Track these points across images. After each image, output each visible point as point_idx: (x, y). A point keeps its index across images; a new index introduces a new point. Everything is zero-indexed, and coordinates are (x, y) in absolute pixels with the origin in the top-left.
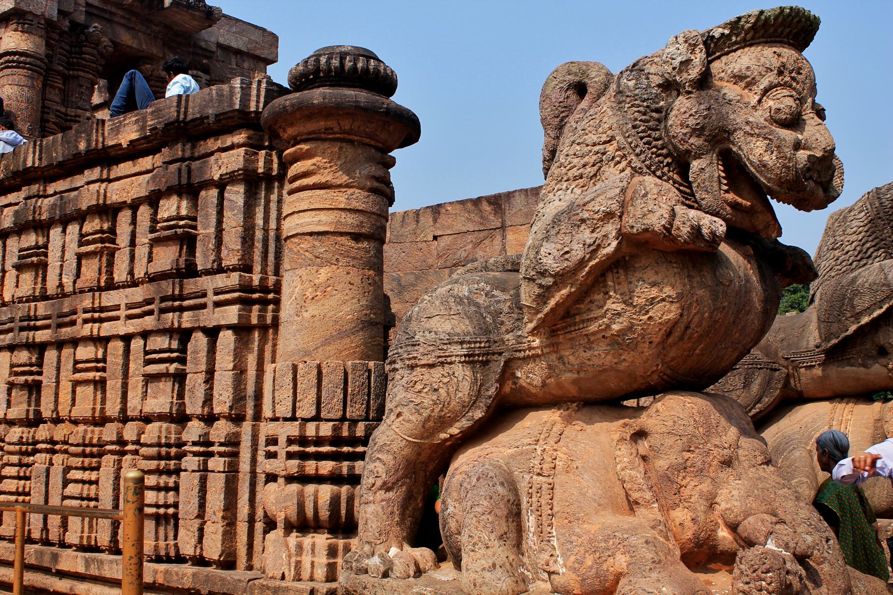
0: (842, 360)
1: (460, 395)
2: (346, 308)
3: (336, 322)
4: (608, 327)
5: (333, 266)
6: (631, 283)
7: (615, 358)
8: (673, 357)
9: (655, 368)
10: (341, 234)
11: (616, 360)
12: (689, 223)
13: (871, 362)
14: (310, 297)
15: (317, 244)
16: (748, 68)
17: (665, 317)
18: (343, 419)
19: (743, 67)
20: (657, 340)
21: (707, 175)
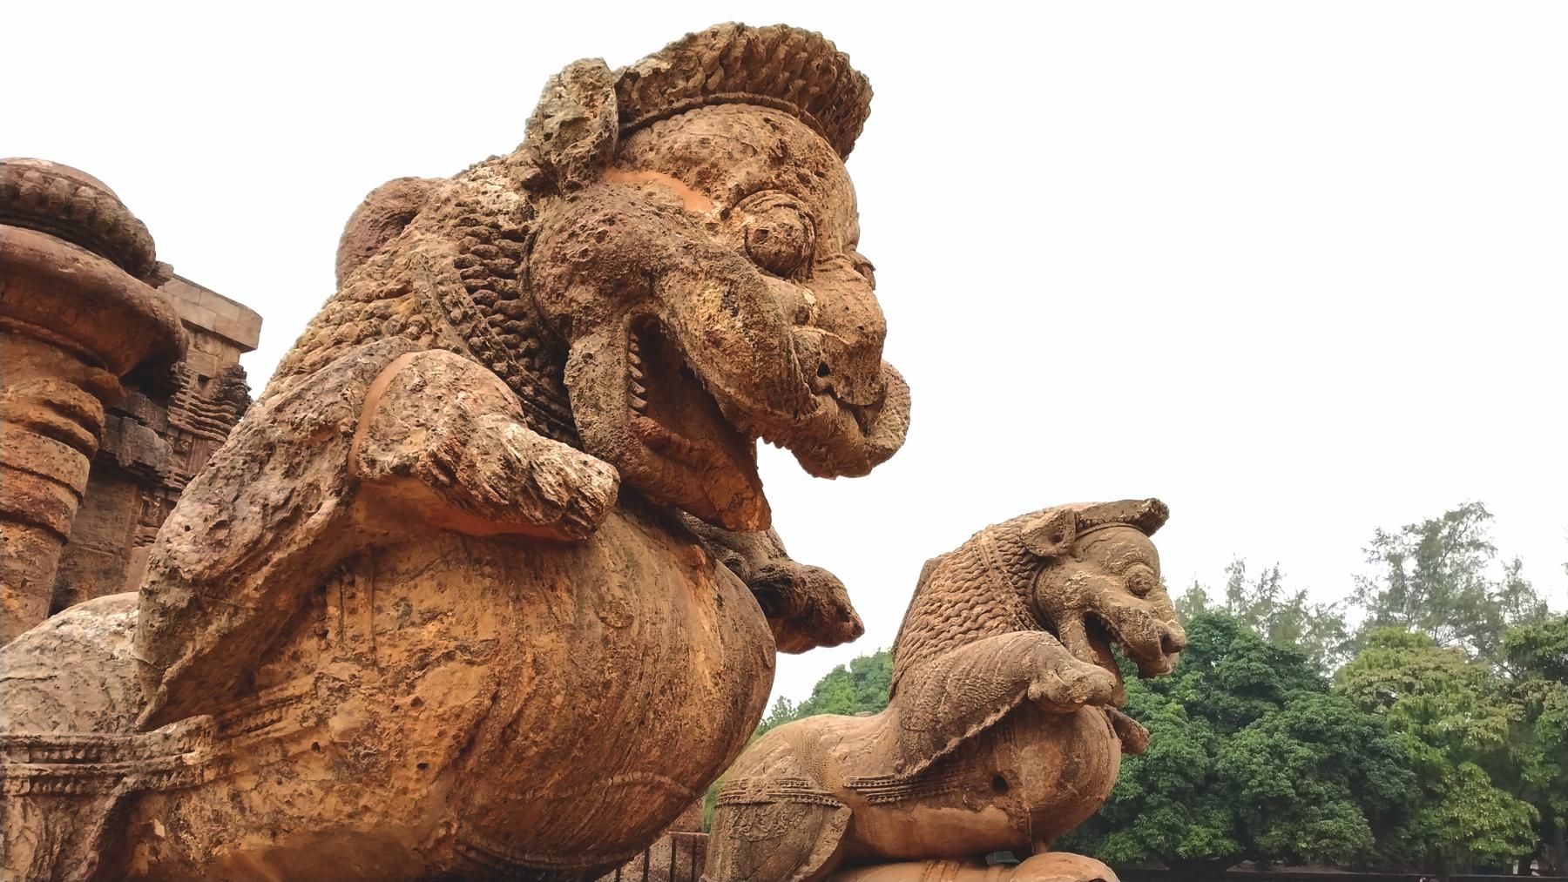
0: (937, 795)
4: (322, 720)
6: (380, 610)
7: (345, 803)
8: (482, 807)
9: (442, 832)
11: (348, 809)
12: (497, 454)
13: (982, 802)
16: (704, 142)
17: (452, 702)
19: (694, 139)
20: (437, 760)
21: (600, 370)
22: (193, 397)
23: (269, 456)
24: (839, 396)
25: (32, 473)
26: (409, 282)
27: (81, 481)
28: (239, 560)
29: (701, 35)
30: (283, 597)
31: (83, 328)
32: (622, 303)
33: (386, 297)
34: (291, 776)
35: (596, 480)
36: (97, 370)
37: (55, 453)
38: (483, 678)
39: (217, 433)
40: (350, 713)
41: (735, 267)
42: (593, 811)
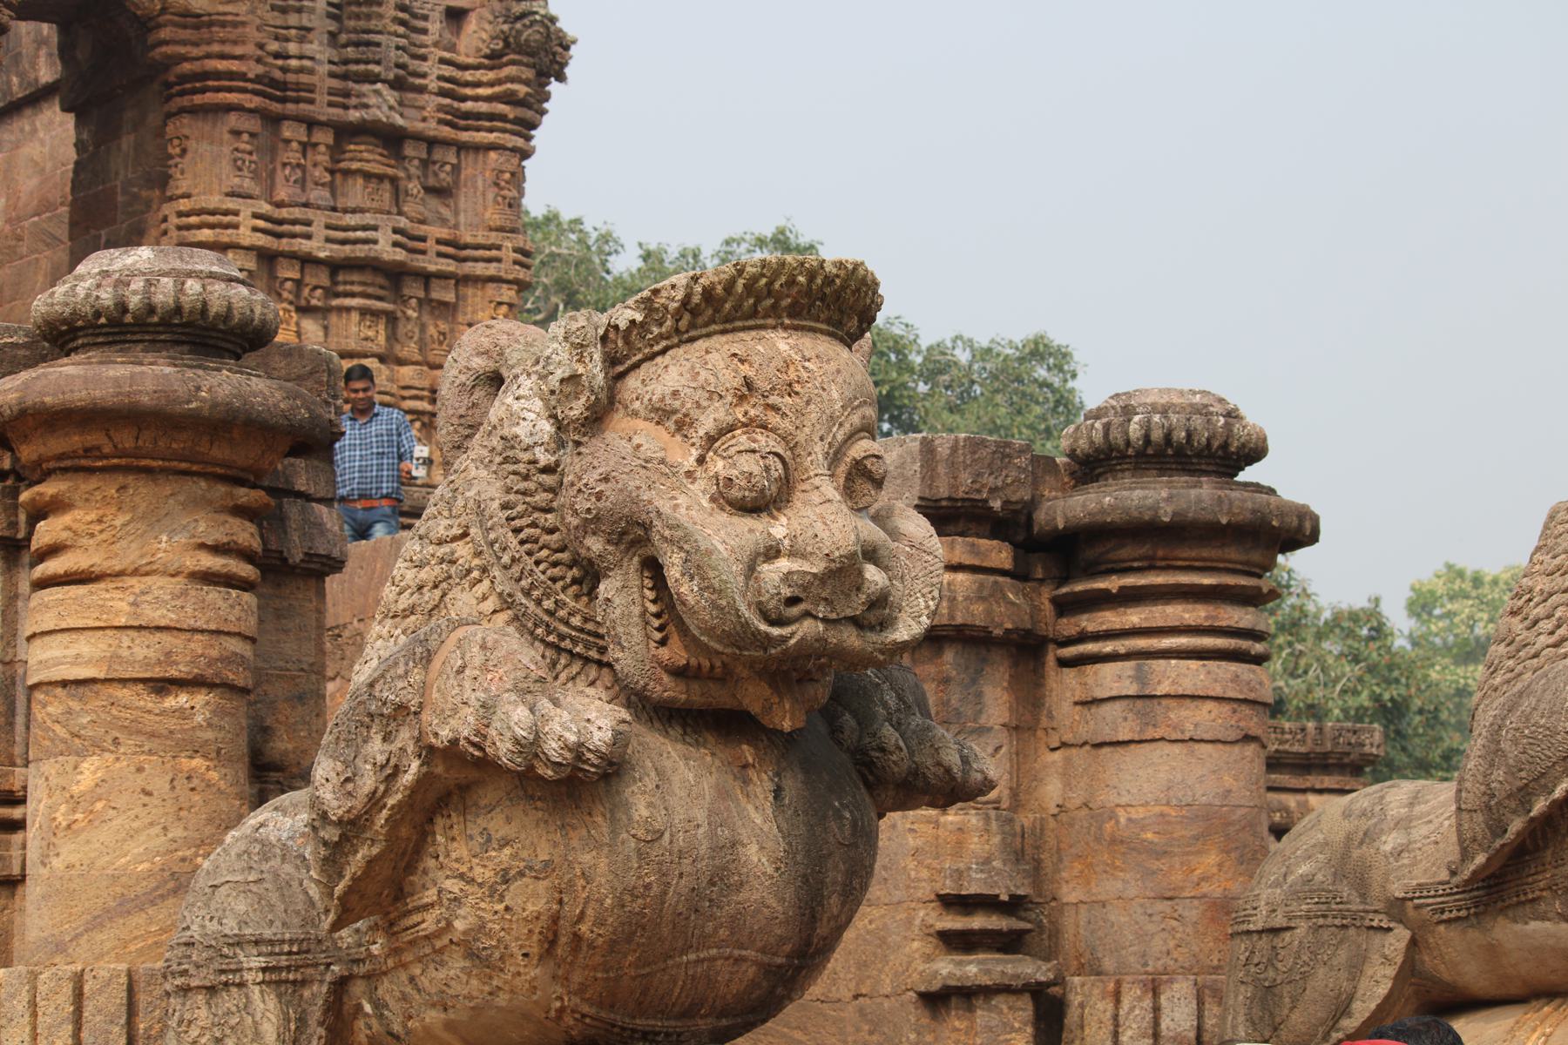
3: (115, 878)
5: (107, 755)
6: (471, 837)
9: (558, 1004)
10: (123, 682)
11: (487, 988)
12: (509, 734)
14: (64, 824)
15: (75, 705)
16: (675, 393)
19: (668, 391)
20: (535, 951)
21: (618, 611)
22: (442, 61)
25: (202, 631)
30: (403, 830)
31: (219, 452)
32: (628, 550)
34: (442, 964)
35: (597, 735)
37: (220, 603)
39: (504, 131)
40: (465, 918)
42: (681, 983)
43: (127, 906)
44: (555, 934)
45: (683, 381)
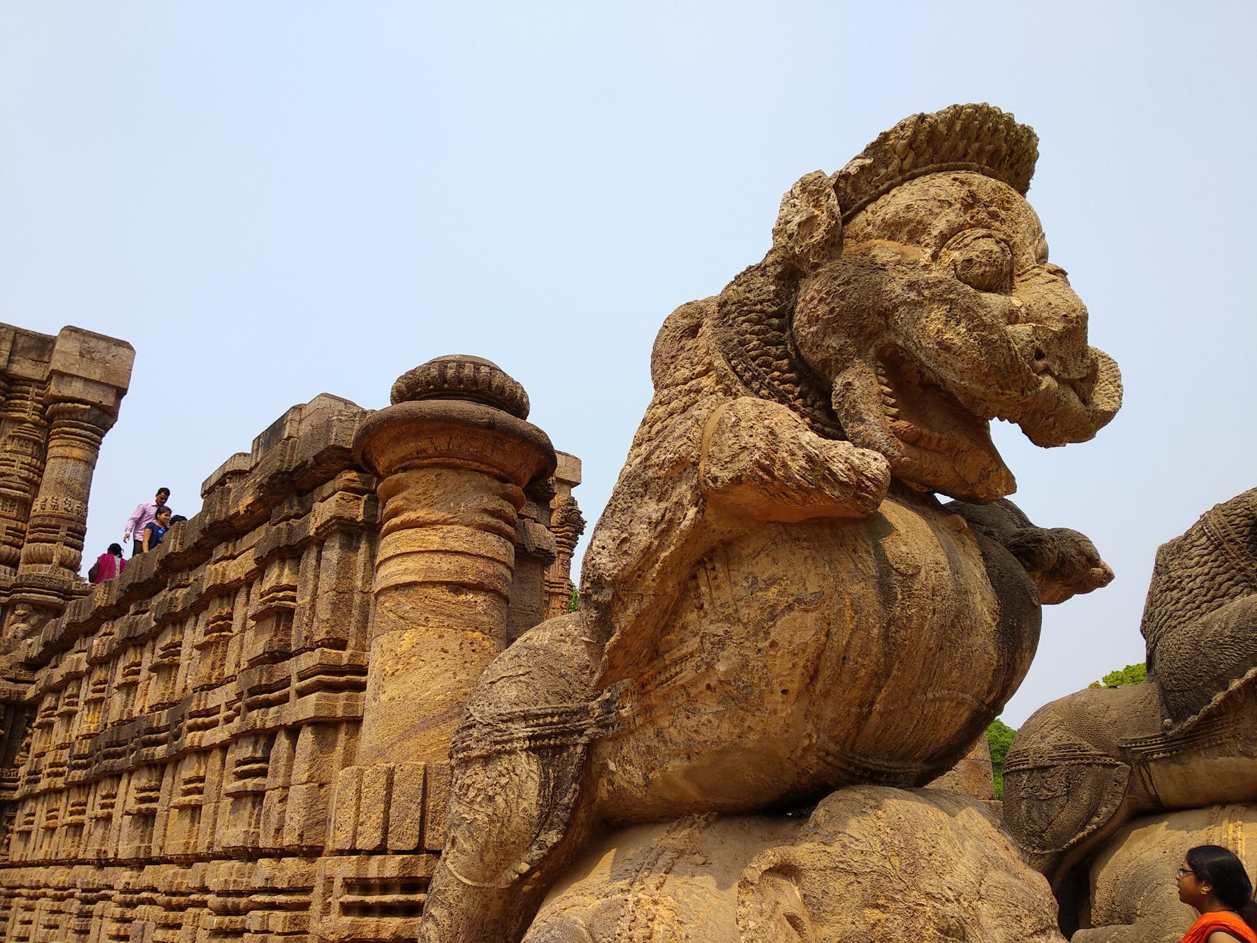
1: (525, 804)
2: (435, 686)
4: (710, 666)
5: (421, 628)
6: (735, 584)
7: (735, 726)
8: (833, 720)
9: (806, 742)
10: (434, 584)
12: (800, 453)
14: (390, 672)
15: (403, 600)
16: (908, 207)
17: (797, 641)
18: (417, 851)
20: (794, 687)
23: (646, 491)
24: (1057, 374)
25: (483, 557)
26: (710, 364)
27: (511, 560)
28: (639, 562)
29: (892, 132)
31: (497, 458)
32: (866, 340)
33: (697, 378)
34: (695, 712)
35: (874, 465)
36: (509, 485)
38: (817, 620)
40: (728, 658)
41: (952, 289)
42: (915, 722)
43: (429, 722)
44: (816, 671)
45: (915, 197)
